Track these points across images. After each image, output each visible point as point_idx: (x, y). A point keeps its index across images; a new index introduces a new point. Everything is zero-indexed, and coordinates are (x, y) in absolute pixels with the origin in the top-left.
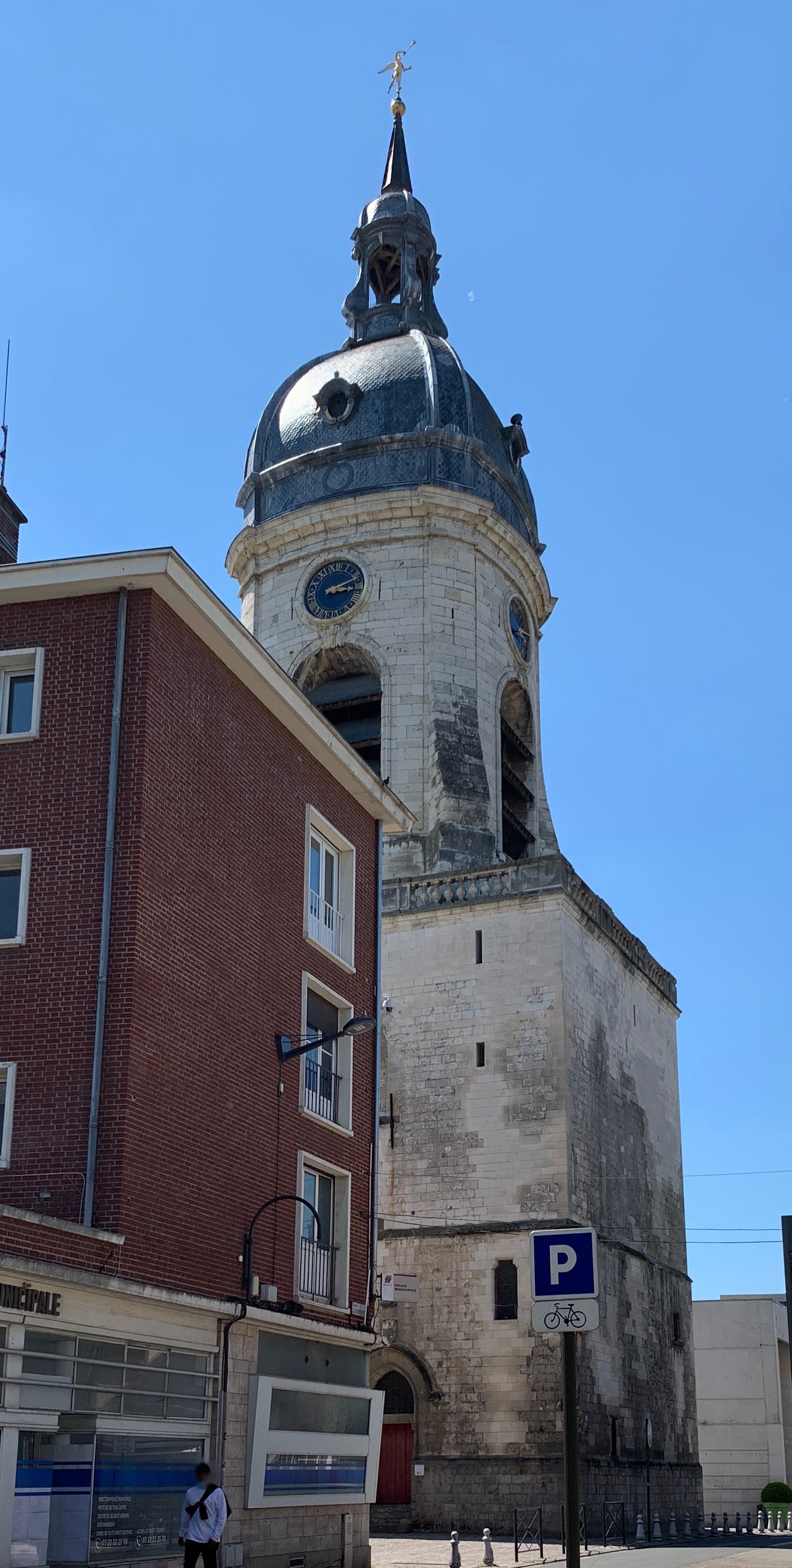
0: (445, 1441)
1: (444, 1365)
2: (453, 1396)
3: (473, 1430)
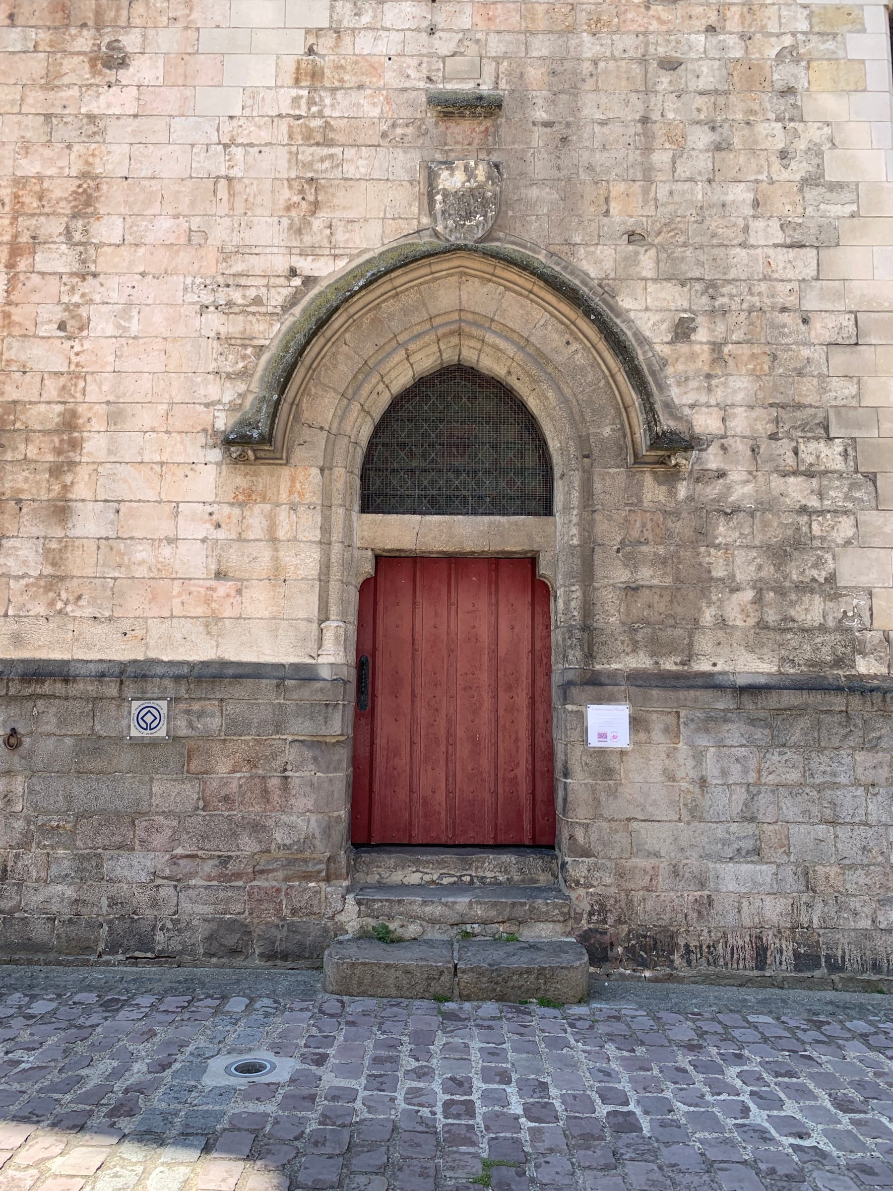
0: (708, 616)
1: (702, 335)
2: (741, 447)
3: (831, 578)
